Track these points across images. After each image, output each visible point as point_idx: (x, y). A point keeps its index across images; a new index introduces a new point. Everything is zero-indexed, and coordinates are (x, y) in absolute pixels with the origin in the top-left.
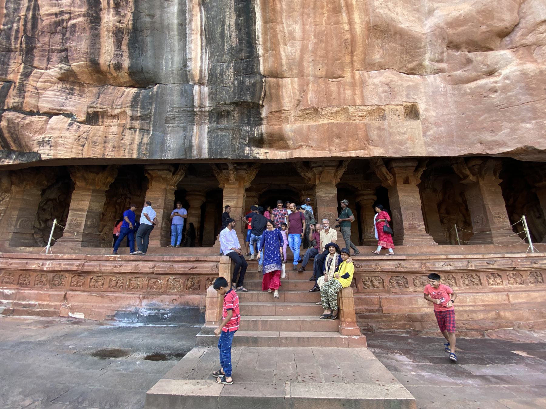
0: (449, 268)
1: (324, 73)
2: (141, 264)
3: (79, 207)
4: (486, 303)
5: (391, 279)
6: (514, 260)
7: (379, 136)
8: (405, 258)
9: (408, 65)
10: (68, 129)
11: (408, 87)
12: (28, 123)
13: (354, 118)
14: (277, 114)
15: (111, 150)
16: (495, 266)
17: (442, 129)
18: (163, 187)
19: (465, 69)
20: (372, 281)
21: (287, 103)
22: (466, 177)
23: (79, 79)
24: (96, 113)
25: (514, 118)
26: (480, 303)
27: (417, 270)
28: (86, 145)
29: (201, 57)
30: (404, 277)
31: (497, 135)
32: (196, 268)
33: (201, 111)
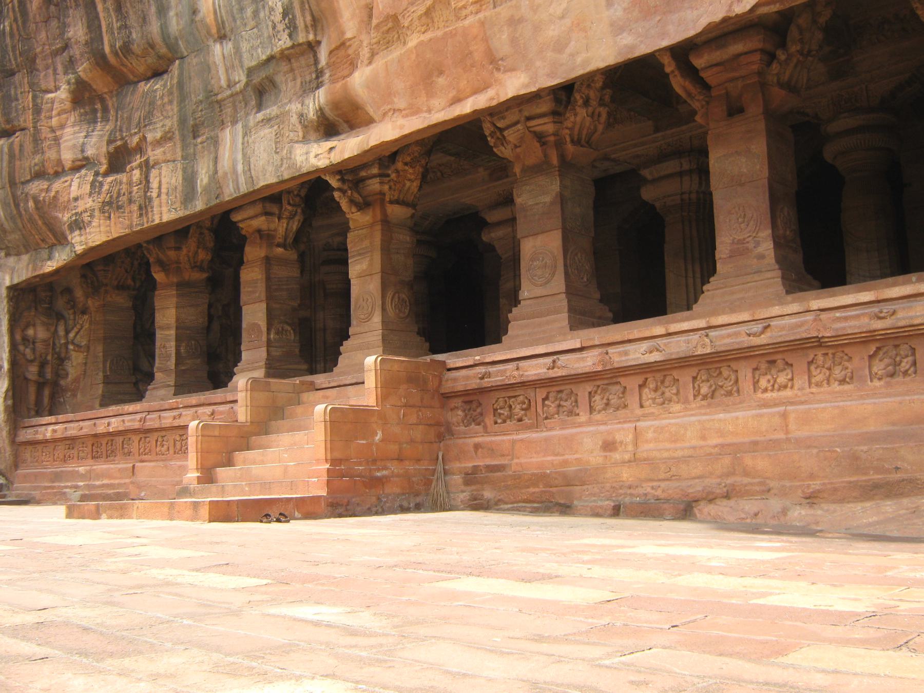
0: (655, 357)
4: (729, 440)
5: (546, 398)
7: (514, 41)
8: (578, 346)
12: (54, 197)
13: (464, 12)
14: (342, 53)
16: (763, 339)
20: (510, 407)
23: (95, 91)
24: (117, 149)
26: (715, 441)
27: (587, 370)
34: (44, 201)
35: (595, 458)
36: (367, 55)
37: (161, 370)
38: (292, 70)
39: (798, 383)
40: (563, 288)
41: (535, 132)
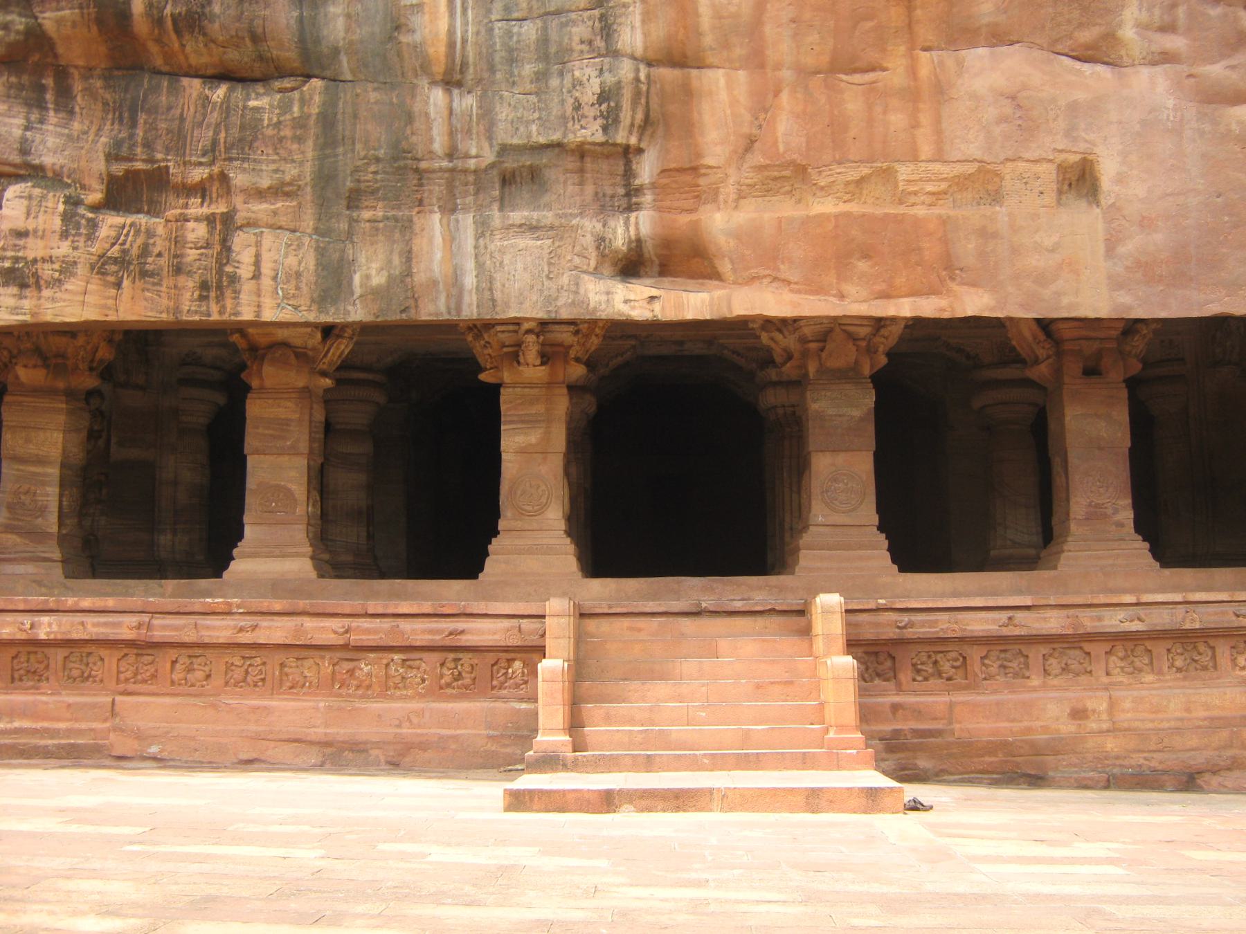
0: (1136, 626)
1: (825, 59)
2: (309, 623)
3: (32, 449)
4: (1216, 713)
8: (1029, 603)
9: (1076, 34)
10: (64, 235)
11: (1073, 107)
13: (912, 199)
15: (196, 294)
17: (1159, 237)
19: (1233, 62)
20: (936, 662)
23: (56, 56)
24: (132, 175)
27: (1054, 632)
28: (126, 283)
30: (1020, 652)
32: (462, 632)
33: (452, 170)
35: (1067, 728)
36: (733, 196)
38: (582, 171)
40: (875, 519)
41: (845, 331)
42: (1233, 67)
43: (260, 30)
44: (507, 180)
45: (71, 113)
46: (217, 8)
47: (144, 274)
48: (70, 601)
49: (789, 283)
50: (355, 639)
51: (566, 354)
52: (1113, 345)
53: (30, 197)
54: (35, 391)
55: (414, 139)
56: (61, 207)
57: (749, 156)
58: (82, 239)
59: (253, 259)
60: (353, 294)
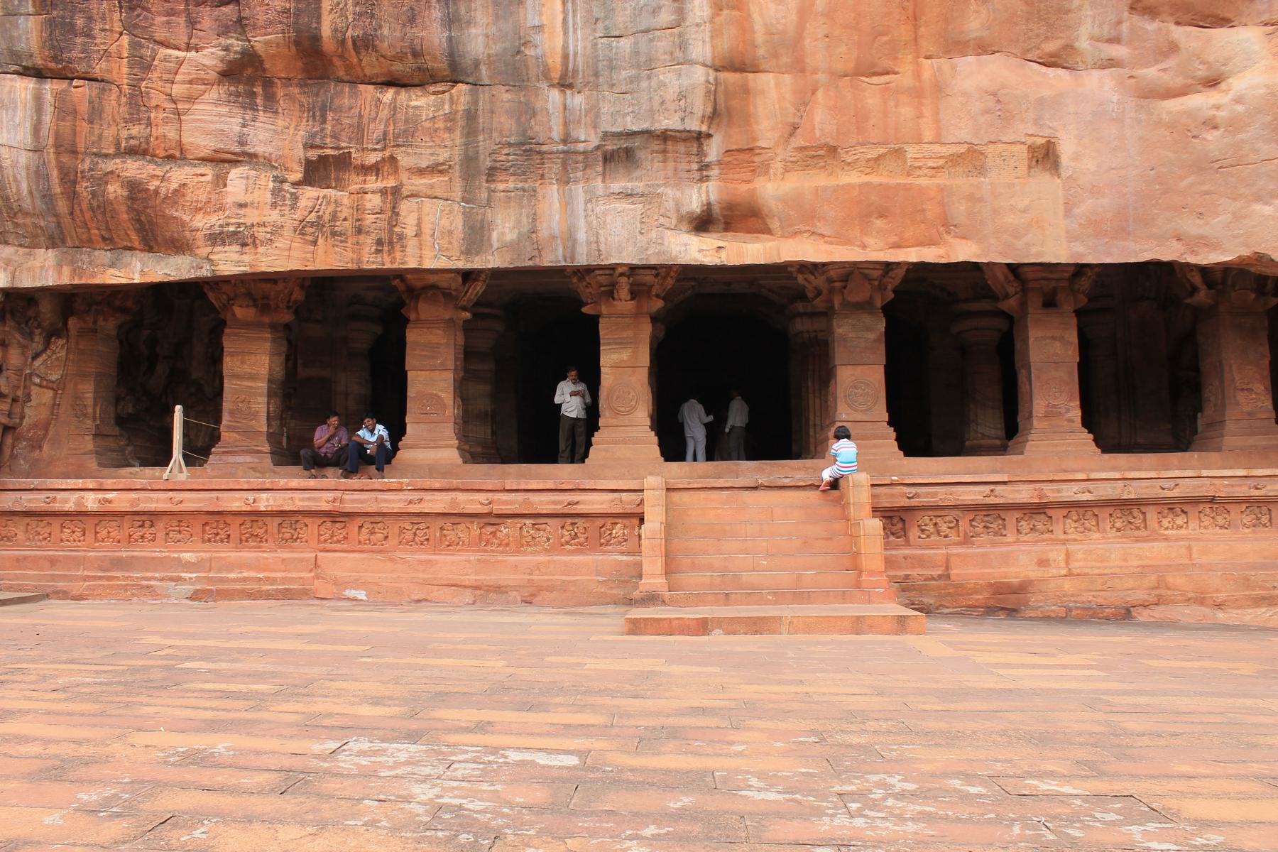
0: (1087, 497)
1: (852, 65)
2: (461, 496)
3: (246, 369)
4: (1146, 562)
6: (1216, 481)
10: (274, 205)
11: (1041, 102)
12: (176, 190)
13: (918, 172)
14: (741, 156)
15: (373, 249)
16: (1175, 493)
17: (1105, 201)
18: (447, 314)
19: (1164, 66)
20: (935, 524)
21: (766, 131)
22: (1194, 290)
23: (264, 70)
24: (323, 159)
25: (1242, 190)
28: (321, 241)
29: (565, 21)
31: (1207, 224)
34: (157, 192)
35: (1033, 573)
36: (781, 170)
37: (231, 429)
38: (664, 152)
39: (1191, 525)
40: (886, 417)
42: (1164, 70)
43: (418, 48)
44: (609, 158)
45: (276, 113)
46: (386, 32)
47: (334, 234)
48: (282, 483)
49: (824, 236)
50: (496, 508)
51: (649, 291)
52: (1065, 284)
53: (248, 178)
54: (248, 325)
55: (536, 128)
56: (271, 185)
57: (792, 139)
58: (287, 208)
59: (415, 222)
60: (491, 246)
